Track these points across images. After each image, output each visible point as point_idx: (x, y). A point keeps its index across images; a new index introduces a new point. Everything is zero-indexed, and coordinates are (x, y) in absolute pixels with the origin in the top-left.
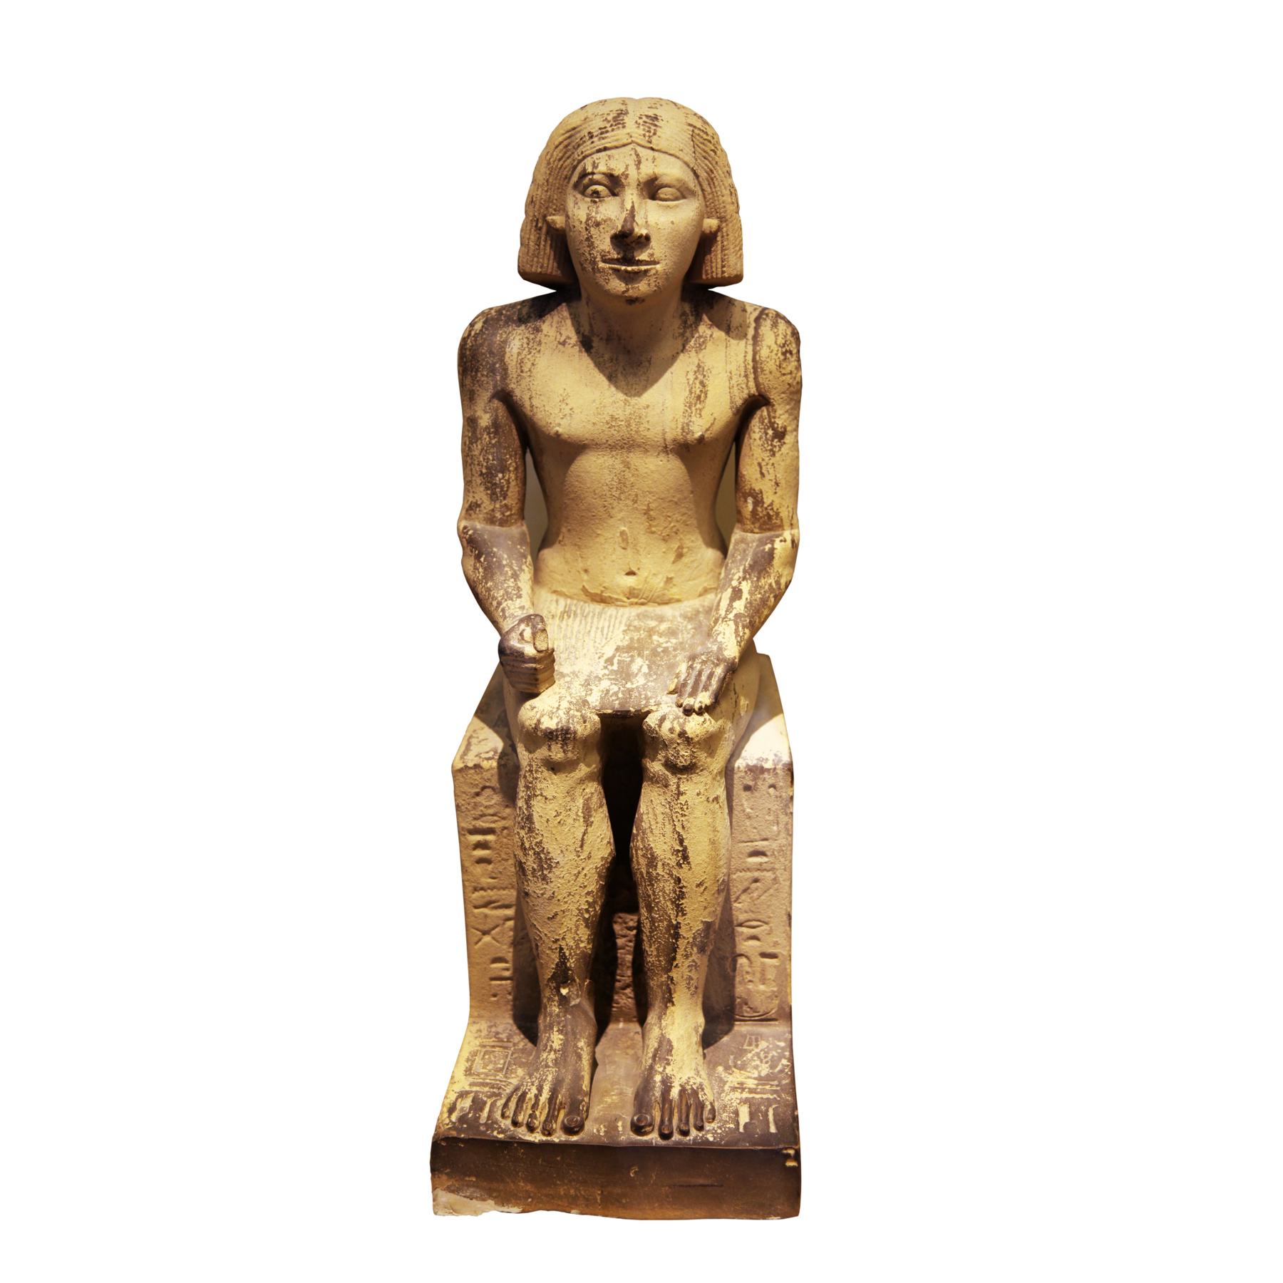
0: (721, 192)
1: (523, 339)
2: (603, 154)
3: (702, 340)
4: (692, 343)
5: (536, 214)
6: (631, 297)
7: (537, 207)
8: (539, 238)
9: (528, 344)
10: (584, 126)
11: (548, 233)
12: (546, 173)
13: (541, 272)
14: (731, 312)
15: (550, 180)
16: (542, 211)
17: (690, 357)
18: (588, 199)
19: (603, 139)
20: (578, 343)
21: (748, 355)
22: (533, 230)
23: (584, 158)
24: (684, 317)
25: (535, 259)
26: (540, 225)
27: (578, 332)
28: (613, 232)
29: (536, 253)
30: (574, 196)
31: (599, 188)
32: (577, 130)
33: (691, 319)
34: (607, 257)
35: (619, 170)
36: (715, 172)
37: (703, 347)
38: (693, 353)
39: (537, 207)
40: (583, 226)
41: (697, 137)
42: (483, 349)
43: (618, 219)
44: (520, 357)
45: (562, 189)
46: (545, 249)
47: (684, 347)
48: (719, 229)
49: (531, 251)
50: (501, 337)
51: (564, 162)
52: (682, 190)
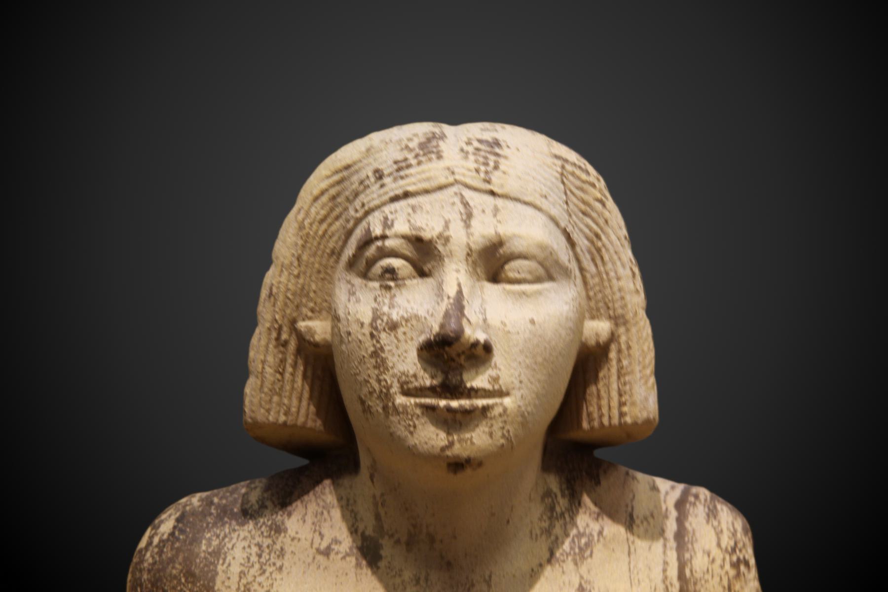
0: (616, 273)
1: (249, 546)
2: (402, 203)
3: (583, 541)
4: (566, 546)
5: (277, 317)
6: (457, 457)
7: (279, 304)
8: (283, 361)
9: (260, 556)
10: (365, 161)
11: (299, 351)
12: (296, 244)
13: (285, 423)
14: (632, 491)
15: (305, 257)
16: (288, 311)
17: (563, 572)
18: (376, 284)
19: (402, 178)
20: (355, 551)
21: (669, 569)
22: (271, 346)
23: (367, 213)
24: (548, 501)
25: (276, 399)
26: (284, 336)
27: (353, 530)
28: (422, 338)
29: (277, 387)
30: (349, 282)
31: (396, 263)
32: (353, 169)
33: (562, 503)
34: (411, 386)
35: (433, 229)
36: (603, 237)
37: (588, 553)
38: (569, 565)
39: (279, 304)
40: (367, 330)
41: (571, 178)
42: (173, 568)
43: (432, 315)
44: (244, 581)
45: (326, 273)
46: (293, 381)
47: (552, 553)
48: (613, 337)
49: (267, 384)
50: (209, 544)
51: (330, 225)
52: (548, 264)
